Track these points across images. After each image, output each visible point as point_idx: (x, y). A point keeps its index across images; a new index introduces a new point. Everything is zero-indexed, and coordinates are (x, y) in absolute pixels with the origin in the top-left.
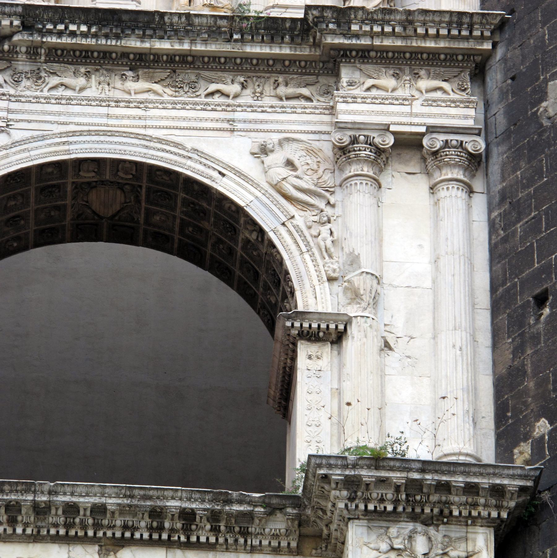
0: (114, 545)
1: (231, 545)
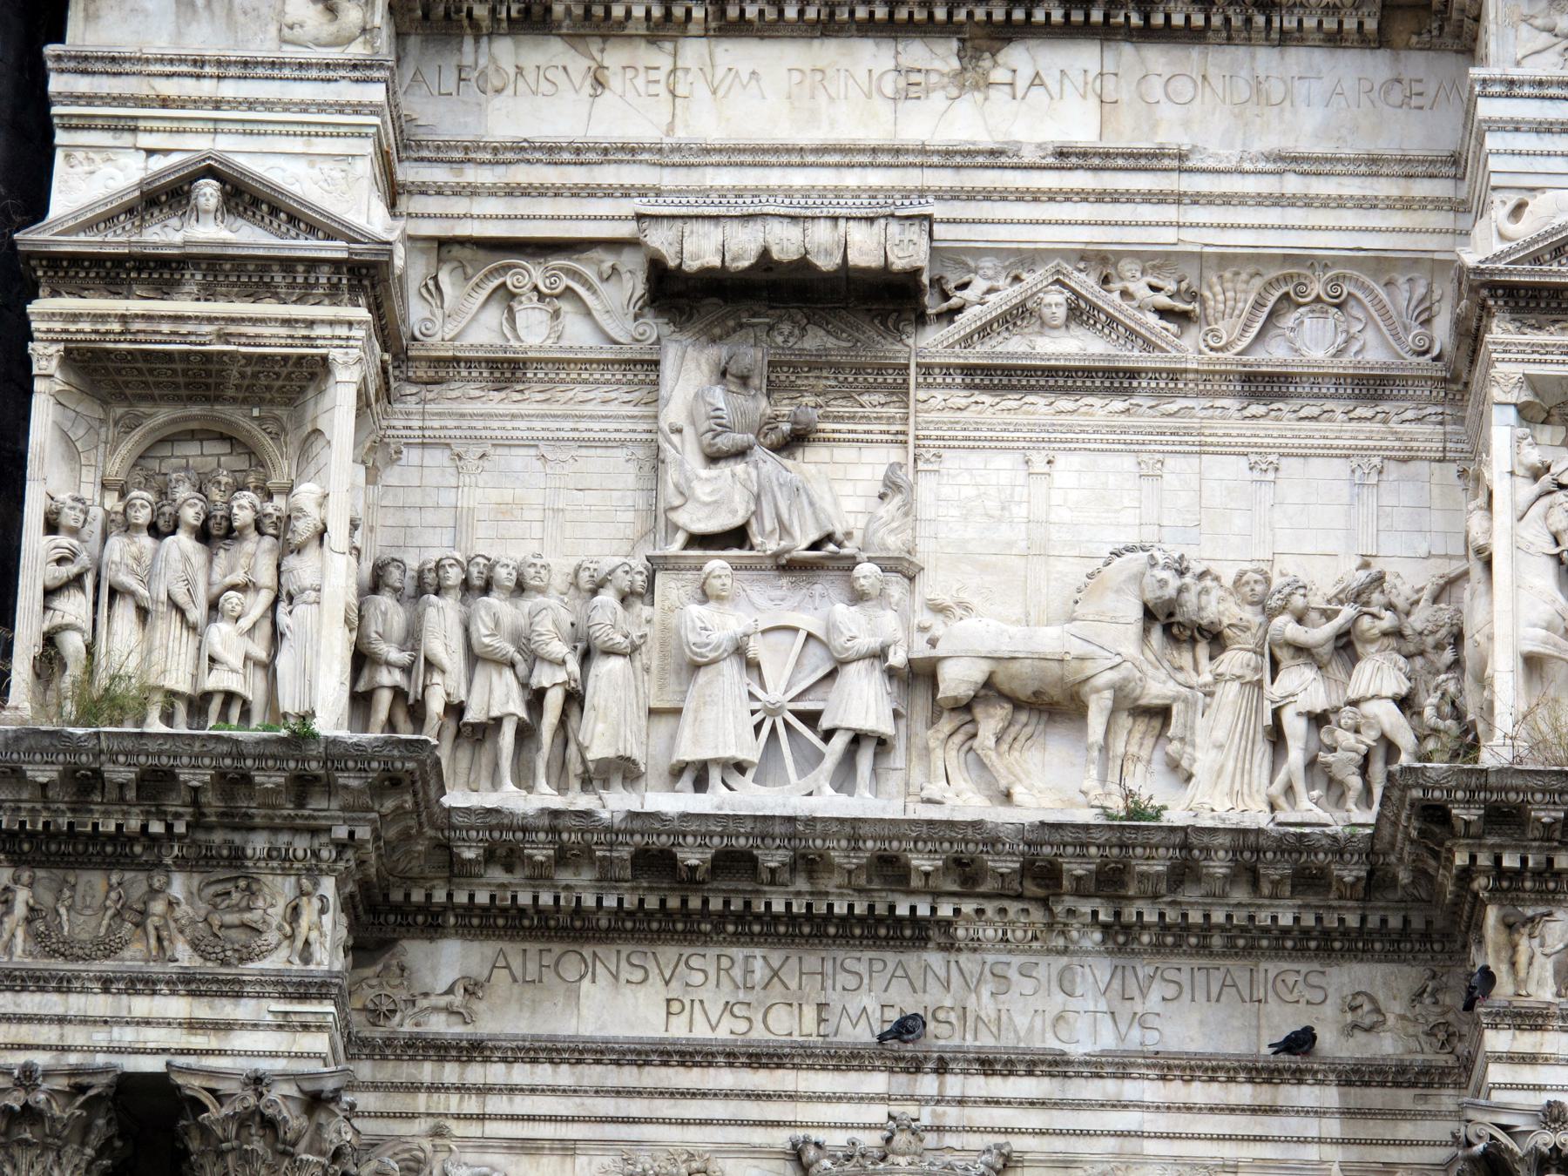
0: (991, 38)
1: (1239, 31)
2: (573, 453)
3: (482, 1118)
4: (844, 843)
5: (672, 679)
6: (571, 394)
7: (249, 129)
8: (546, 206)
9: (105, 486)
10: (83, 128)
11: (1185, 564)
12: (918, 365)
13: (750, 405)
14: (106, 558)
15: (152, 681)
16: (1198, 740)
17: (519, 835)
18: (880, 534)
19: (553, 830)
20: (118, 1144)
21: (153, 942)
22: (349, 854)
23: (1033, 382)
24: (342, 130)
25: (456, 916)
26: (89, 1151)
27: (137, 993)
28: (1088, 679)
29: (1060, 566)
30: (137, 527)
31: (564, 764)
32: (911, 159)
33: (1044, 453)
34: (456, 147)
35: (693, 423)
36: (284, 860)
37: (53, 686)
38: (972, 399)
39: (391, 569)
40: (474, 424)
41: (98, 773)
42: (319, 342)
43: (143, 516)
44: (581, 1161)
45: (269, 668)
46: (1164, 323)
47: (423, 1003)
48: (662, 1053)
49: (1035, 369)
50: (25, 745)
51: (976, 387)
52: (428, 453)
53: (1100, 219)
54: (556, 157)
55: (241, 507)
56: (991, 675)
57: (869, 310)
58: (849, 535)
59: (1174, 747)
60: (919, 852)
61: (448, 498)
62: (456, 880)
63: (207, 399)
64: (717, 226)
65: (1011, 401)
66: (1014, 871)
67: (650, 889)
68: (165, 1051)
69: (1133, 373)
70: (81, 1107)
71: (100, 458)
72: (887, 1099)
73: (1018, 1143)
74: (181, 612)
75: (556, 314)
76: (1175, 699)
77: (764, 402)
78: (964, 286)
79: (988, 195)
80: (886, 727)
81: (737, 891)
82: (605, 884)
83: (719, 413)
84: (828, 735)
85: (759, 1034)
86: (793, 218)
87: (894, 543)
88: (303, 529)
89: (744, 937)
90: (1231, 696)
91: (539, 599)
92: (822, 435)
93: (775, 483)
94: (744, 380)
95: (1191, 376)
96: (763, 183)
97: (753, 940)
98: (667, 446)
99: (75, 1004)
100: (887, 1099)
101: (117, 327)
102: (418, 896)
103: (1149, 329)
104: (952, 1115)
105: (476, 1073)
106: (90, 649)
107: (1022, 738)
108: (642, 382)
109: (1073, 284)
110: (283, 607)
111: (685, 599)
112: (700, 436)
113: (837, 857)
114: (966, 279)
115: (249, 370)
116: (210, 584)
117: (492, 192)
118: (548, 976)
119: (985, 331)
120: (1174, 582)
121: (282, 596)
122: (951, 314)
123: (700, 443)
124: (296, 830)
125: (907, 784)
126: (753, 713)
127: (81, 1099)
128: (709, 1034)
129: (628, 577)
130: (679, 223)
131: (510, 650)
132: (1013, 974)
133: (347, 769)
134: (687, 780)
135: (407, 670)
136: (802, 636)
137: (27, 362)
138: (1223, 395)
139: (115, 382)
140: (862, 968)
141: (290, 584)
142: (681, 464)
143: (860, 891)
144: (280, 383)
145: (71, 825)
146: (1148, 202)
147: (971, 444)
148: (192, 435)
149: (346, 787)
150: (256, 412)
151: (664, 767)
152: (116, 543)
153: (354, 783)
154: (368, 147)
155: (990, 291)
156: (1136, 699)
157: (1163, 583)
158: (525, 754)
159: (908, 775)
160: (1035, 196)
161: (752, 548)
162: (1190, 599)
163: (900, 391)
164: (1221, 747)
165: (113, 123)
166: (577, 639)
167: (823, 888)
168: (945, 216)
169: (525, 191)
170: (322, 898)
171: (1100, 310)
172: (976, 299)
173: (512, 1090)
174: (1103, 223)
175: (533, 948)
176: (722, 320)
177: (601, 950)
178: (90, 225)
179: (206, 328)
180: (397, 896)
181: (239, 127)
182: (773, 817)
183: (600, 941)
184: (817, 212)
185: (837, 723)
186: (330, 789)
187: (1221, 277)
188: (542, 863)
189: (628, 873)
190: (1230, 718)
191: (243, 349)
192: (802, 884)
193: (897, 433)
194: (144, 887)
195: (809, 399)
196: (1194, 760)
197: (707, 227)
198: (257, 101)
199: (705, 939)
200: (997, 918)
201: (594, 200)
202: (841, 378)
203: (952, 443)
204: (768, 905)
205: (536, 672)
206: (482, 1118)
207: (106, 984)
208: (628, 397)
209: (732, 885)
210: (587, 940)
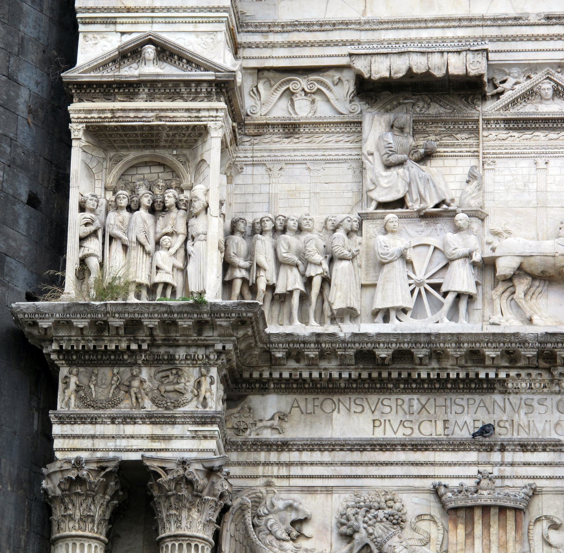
2: (323, 166)
3: (288, 477)
4: (454, 345)
5: (372, 270)
6: (321, 139)
7: (168, 21)
8: (307, 51)
9: (106, 189)
10: (91, 23)
12: (483, 119)
13: (405, 141)
14: (107, 222)
15: (131, 278)
17: (302, 345)
18: (467, 199)
19: (318, 342)
20: (121, 493)
21: (134, 400)
22: (223, 356)
23: (537, 126)
24: (211, 20)
25: (274, 384)
26: (107, 497)
27: (127, 423)
30: (122, 208)
31: (322, 312)
32: (477, 23)
34: (264, 26)
35: (378, 150)
36: (193, 360)
37: (85, 282)
38: (509, 135)
39: (240, 223)
40: (276, 154)
41: (106, 322)
42: (203, 119)
43: (124, 202)
44: (335, 496)
45: (184, 271)
47: (260, 424)
48: (371, 445)
49: (538, 119)
50: (72, 310)
51: (511, 129)
52: (256, 168)
54: (311, 28)
55: (169, 197)
56: (521, 264)
57: (460, 95)
58: (453, 200)
60: (489, 348)
61: (265, 189)
62: (273, 367)
63: (152, 147)
64: (387, 58)
65: (527, 135)
66: (534, 356)
67: (364, 369)
68: (141, 450)
70: (103, 477)
71: (104, 176)
72: (477, 464)
73: (539, 483)
74: (143, 246)
75: (313, 102)
77: (411, 140)
78: (504, 82)
79: (514, 39)
80: (472, 290)
81: (404, 369)
82: (343, 367)
83: (390, 145)
84: (445, 294)
85: (416, 435)
86: (423, 53)
87: (474, 204)
88: (198, 206)
89: (408, 390)
91: (309, 235)
92: (439, 154)
93: (417, 177)
94: (402, 129)
96: (408, 37)
97: (412, 391)
98: (366, 161)
99: (99, 429)
100: (477, 464)
101: (109, 115)
102: (256, 375)
104: (508, 471)
105: (285, 457)
106: (102, 265)
107: (537, 293)
108: (354, 132)
109: (555, 79)
110: (189, 243)
111: (377, 233)
113: (450, 351)
114: (505, 78)
115: (171, 133)
116: (156, 233)
117: (282, 45)
118: (318, 411)
119: (514, 102)
121: (189, 238)
122: (498, 95)
123: (382, 159)
124: (198, 346)
125: (483, 316)
126: (410, 285)
127: (103, 473)
128: (393, 436)
129: (350, 223)
131: (296, 259)
132: (535, 404)
133: (221, 317)
134: (380, 317)
135: (248, 270)
136: (432, 248)
137: (69, 133)
139: (110, 141)
140: (464, 403)
141: (192, 232)
142: (373, 170)
143: (462, 367)
144: (185, 139)
145: (94, 346)
147: (509, 156)
148: (146, 164)
149: (221, 326)
150: (175, 152)
151: (369, 311)
152: (112, 215)
153: (224, 324)
154: (223, 27)
155: (516, 83)
158: (304, 307)
159: (484, 312)
160: (536, 38)
161: (407, 208)
163: (475, 132)
165: (105, 20)
166: (327, 253)
167: (445, 366)
168: (494, 49)
169: (297, 45)
170: (211, 377)
172: (510, 88)
173: (302, 464)
175: (310, 397)
176: (391, 101)
177: (341, 398)
178: (96, 68)
179: (151, 114)
180: (246, 375)
181: (163, 20)
182: (420, 334)
183: (341, 393)
184: (434, 50)
185: (449, 288)
186: (213, 326)
188: (313, 358)
189: (353, 362)
191: (168, 123)
192: (434, 365)
193: (474, 152)
194: (129, 375)
195: (432, 137)
197: (382, 58)
198: (171, 8)
199: (390, 391)
200: (527, 378)
201: (329, 48)
202: (447, 126)
203: (500, 156)
204: (419, 375)
205: (308, 269)
206: (288, 477)
207: (113, 420)
208: (347, 139)
209: (402, 366)
210: (335, 393)
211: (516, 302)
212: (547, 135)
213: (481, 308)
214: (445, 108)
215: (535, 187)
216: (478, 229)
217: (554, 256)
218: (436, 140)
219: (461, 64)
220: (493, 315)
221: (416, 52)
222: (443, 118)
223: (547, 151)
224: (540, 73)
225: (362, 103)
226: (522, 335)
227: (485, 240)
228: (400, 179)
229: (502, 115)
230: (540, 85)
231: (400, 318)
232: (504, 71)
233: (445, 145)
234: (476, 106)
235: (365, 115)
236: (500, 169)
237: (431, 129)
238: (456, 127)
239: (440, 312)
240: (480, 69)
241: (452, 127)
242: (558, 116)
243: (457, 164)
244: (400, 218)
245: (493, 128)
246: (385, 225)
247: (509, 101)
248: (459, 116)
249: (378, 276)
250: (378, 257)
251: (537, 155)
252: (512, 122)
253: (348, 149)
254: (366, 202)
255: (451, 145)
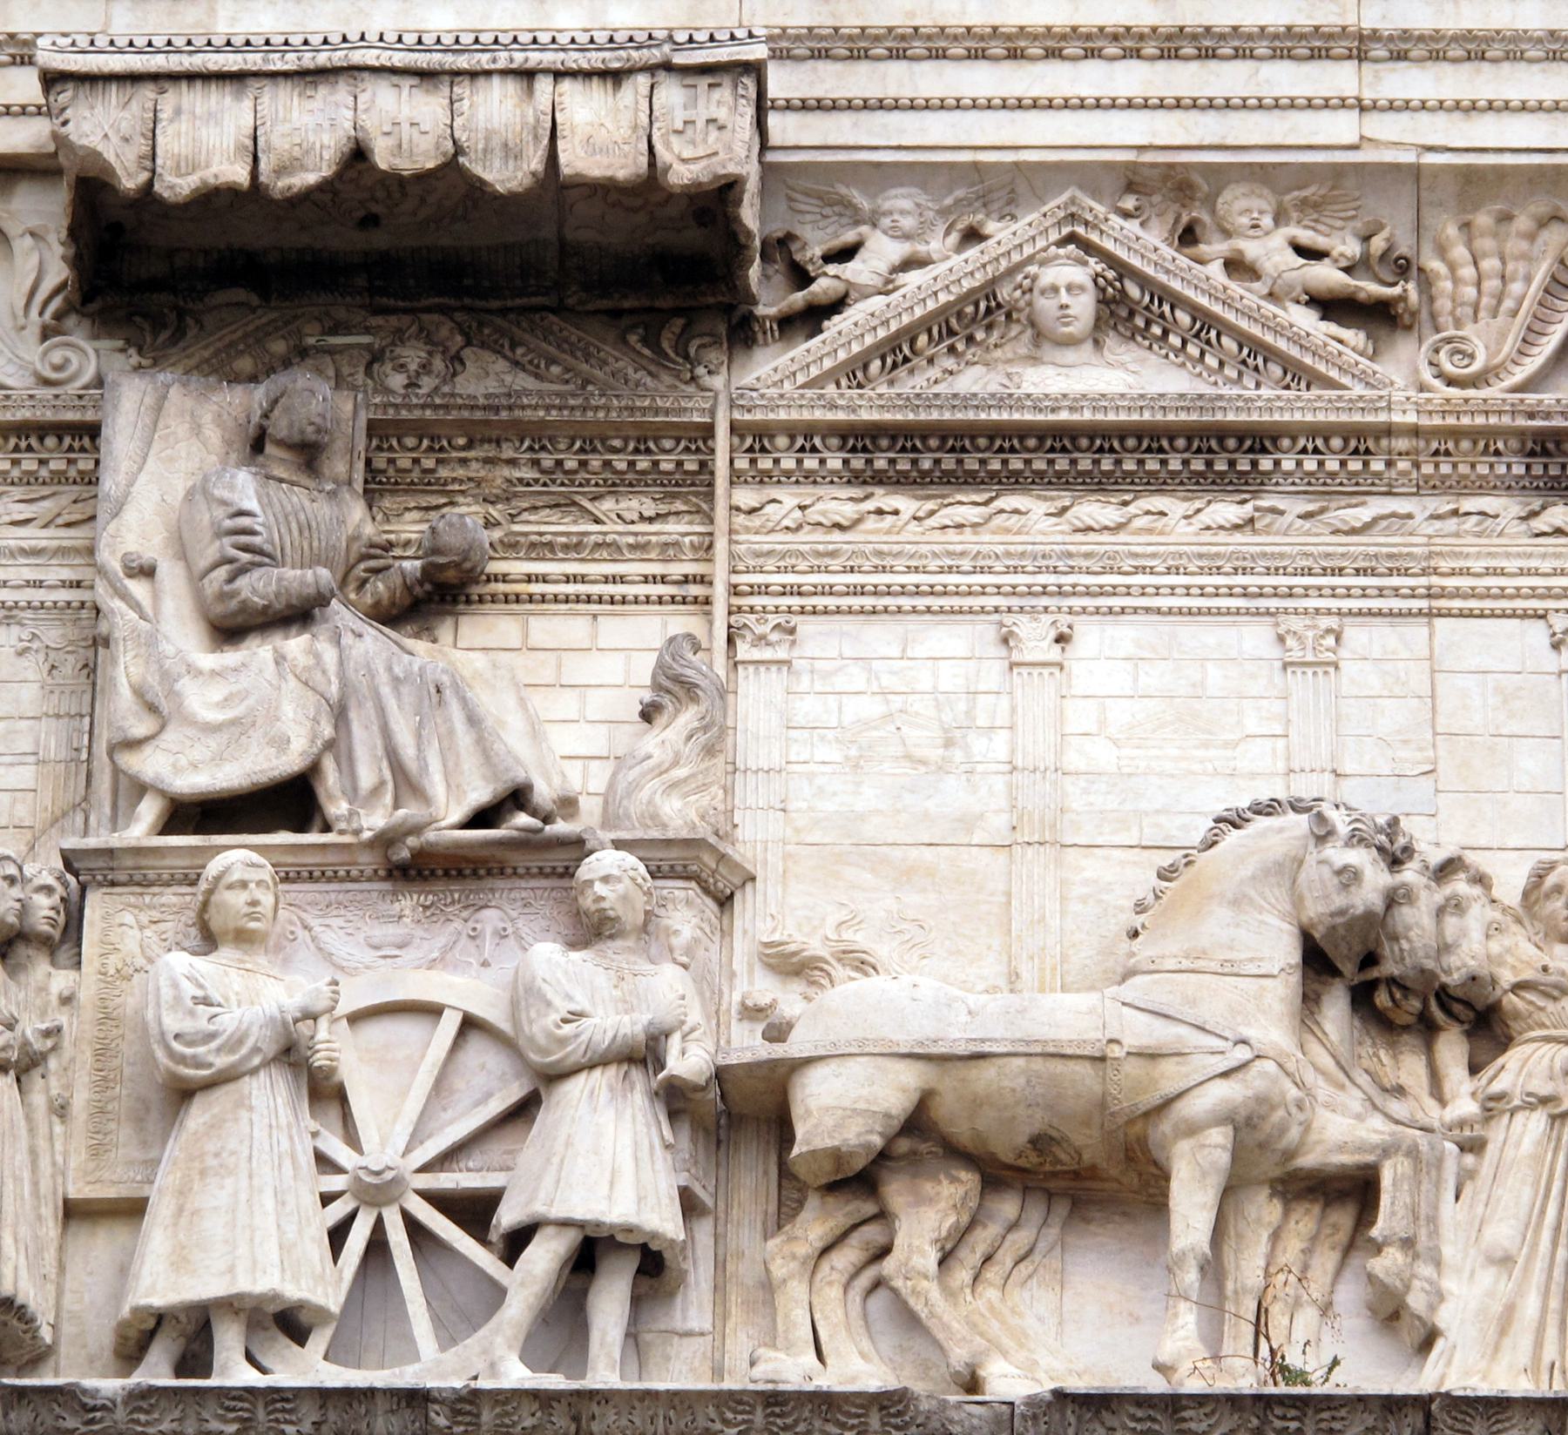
5: (124, 1133)
11: (1401, 841)
12: (734, 428)
13: (322, 510)
16: (1448, 1252)
18: (644, 794)
23: (1016, 464)
28: (1168, 1103)
29: (1091, 867)
33: (1046, 619)
35: (182, 554)
38: (870, 505)
46: (1332, 328)
49: (1021, 432)
51: (879, 479)
53: (1170, 93)
57: (616, 314)
59: (1388, 1263)
64: (238, 96)
65: (964, 508)
69: (1260, 439)
76: (1387, 1151)
77: (356, 511)
78: (846, 254)
80: (664, 1220)
83: (244, 522)
84: (515, 1244)
86: (426, 76)
90: (1527, 1145)
92: (501, 587)
95: (1402, 444)
103: (1295, 340)
107: (1006, 1257)
108: (59, 478)
109: (1109, 245)
112: (197, 579)
114: (849, 236)
120: (1376, 878)
122: (813, 318)
126: (327, 1199)
129: (16, 892)
130: (147, 92)
136: (449, 1024)
138: (1482, 487)
142: (151, 642)
146: (1287, 55)
147: (868, 602)
155: (908, 264)
156: (1289, 1155)
157: (1349, 877)
161: (327, 828)
162: (1417, 921)
164: (1505, 1261)
168: (796, 94)
171: (1177, 301)
172: (877, 282)
174: (1178, 105)
176: (257, 340)
184: (484, 61)
185: (540, 1208)
187: (1466, 226)
190: (1527, 1193)
193: (686, 580)
196: (1440, 1296)
202: (547, 461)
203: (820, 602)
208: (26, 511)
211: (895, 1291)
212: (1064, 510)
213: (708, 1326)
214: (537, 376)
215: (1002, 753)
216: (696, 940)
217: (1103, 1059)
218: (489, 524)
219: (625, 132)
220: (774, 1346)
221: (393, 71)
222: (528, 415)
223: (1067, 580)
224: (1034, 216)
225: (105, 344)
226: (924, 1406)
227: (736, 997)
228: (292, 682)
229: (833, 407)
230: (1032, 269)
231: (265, 1362)
232: (847, 204)
233: (533, 545)
234: (701, 371)
235: (116, 385)
236: (818, 664)
237: (461, 472)
238: (595, 463)
239: (481, 1333)
240: (722, 156)
241: (571, 464)
242: (1123, 417)
243: (594, 636)
244: (286, 879)
245: (788, 474)
246: (205, 905)
247: (869, 340)
248: (608, 409)
249: (157, 1162)
250: (160, 1054)
251: (1015, 602)
252: (884, 443)
253: (24, 552)
254: (107, 810)
255: (566, 547)
